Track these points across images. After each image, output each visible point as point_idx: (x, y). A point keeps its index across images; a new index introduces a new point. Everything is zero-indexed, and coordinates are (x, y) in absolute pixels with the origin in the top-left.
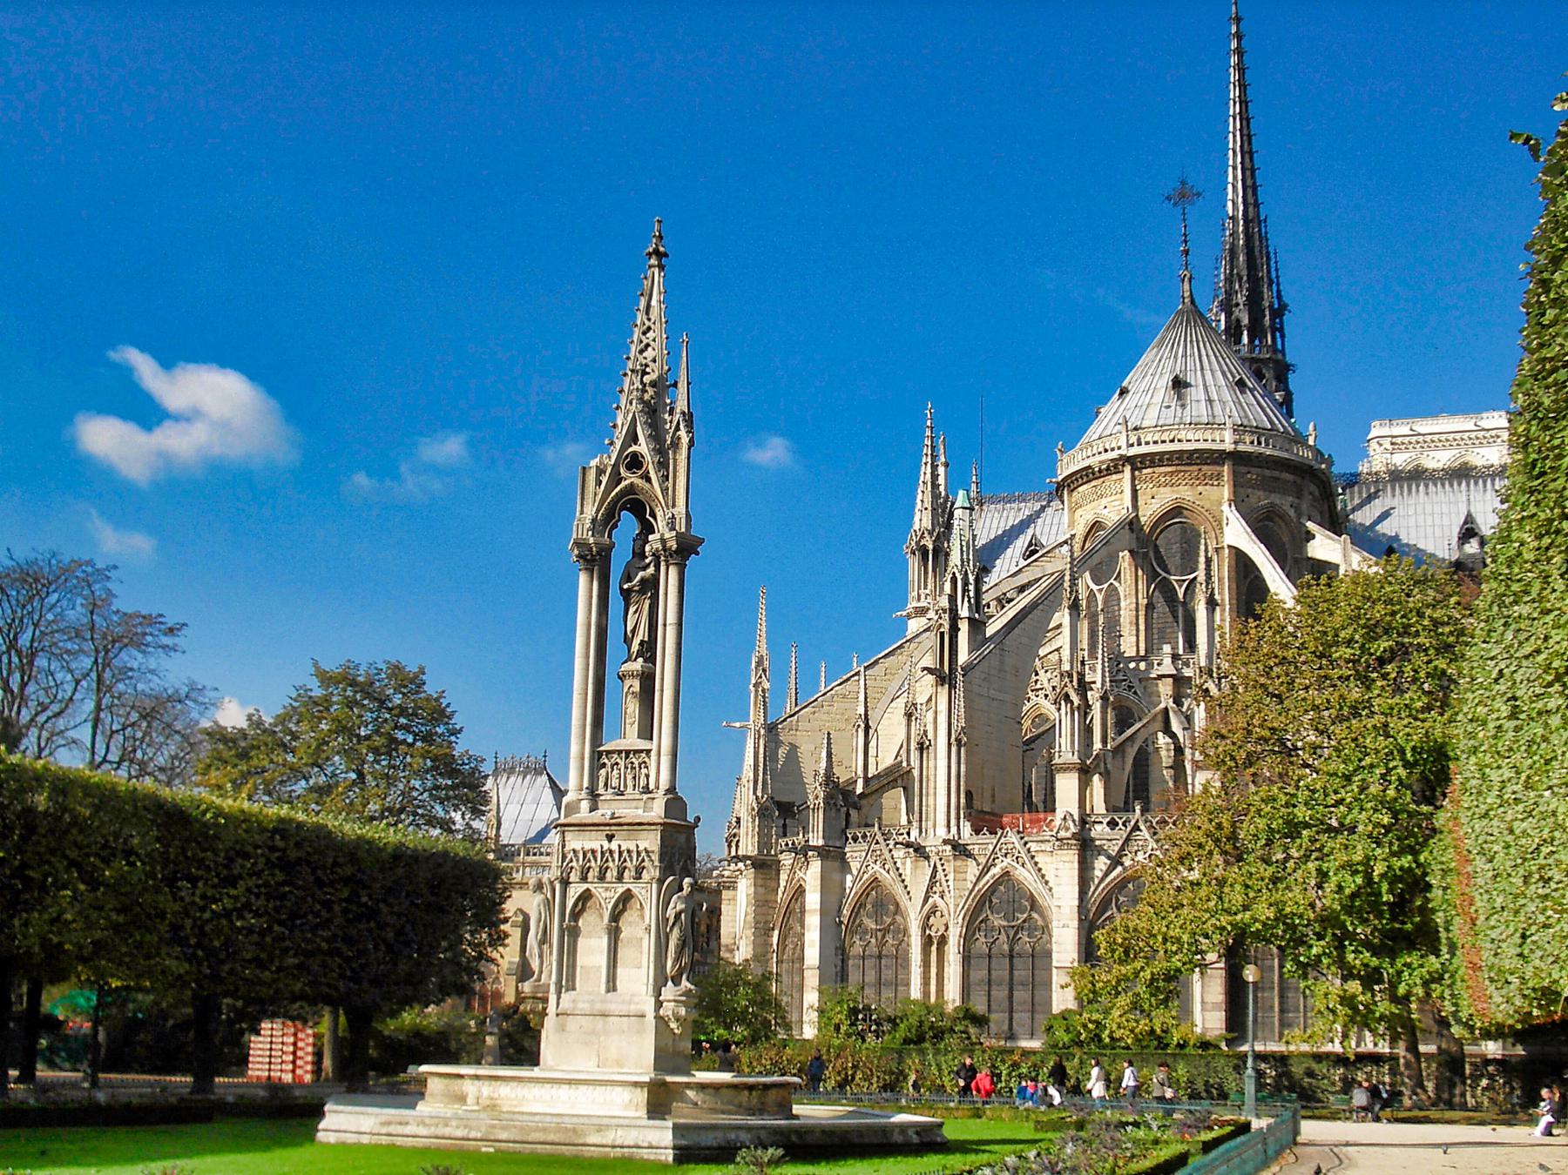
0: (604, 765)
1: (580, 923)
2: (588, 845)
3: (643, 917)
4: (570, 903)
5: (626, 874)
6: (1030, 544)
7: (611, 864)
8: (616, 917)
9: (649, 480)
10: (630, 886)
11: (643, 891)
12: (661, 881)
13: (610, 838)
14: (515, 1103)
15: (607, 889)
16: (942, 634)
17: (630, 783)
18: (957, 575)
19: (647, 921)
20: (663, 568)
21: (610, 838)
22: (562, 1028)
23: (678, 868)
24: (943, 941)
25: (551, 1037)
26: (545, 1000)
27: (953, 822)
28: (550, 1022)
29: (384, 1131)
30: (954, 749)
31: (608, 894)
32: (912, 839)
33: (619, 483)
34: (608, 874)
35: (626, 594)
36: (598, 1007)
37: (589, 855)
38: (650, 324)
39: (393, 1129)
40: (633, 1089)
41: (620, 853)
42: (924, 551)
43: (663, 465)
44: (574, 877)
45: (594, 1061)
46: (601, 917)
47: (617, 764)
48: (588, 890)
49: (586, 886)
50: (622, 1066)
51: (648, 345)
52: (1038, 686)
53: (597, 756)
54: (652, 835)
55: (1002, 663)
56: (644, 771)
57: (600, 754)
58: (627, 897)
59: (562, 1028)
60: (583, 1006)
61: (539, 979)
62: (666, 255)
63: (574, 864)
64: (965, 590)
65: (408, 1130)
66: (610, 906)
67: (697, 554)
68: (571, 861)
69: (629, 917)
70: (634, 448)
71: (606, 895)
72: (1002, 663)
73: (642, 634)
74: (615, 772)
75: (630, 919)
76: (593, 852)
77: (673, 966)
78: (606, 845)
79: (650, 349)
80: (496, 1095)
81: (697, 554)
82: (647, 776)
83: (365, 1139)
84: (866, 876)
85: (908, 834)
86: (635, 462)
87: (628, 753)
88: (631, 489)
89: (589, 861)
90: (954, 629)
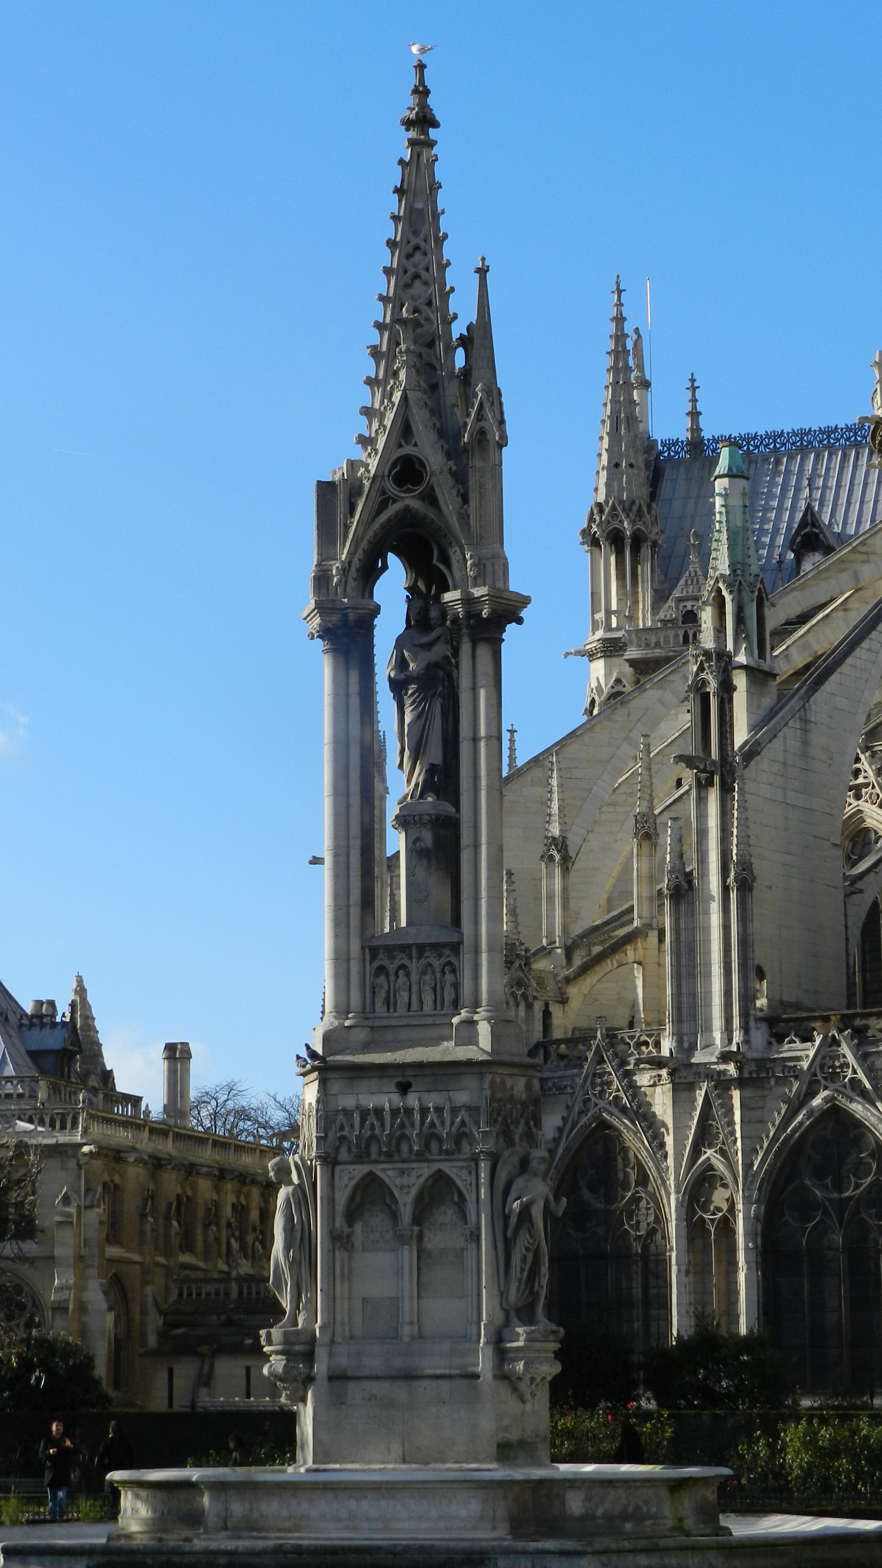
0: (381, 970)
1: (358, 1227)
4: (342, 1198)
5: (434, 1146)
6: (803, 523)
8: (418, 1219)
9: (430, 498)
11: (464, 1174)
12: (495, 1159)
13: (404, 1088)
14: (288, 1525)
15: (402, 1172)
16: (705, 698)
17: (428, 998)
18: (725, 593)
19: (472, 1219)
20: (466, 648)
21: (404, 1088)
23: (518, 1132)
24: (726, 1226)
26: (309, 1357)
27: (736, 1022)
30: (733, 896)
31: (405, 1181)
32: (665, 1052)
34: (405, 1148)
35: (398, 687)
36: (398, 1363)
37: (372, 1119)
38: (414, 241)
41: (424, 1111)
42: (616, 539)
43: (460, 478)
44: (344, 1155)
45: (396, 1449)
46: (394, 1216)
47: (403, 967)
48: (371, 1173)
51: (417, 276)
52: (860, 780)
54: (472, 1082)
55: (805, 743)
56: (449, 978)
57: (374, 952)
58: (440, 1179)
62: (435, 124)
63: (345, 1133)
64: (740, 619)
67: (520, 621)
68: (342, 1128)
69: (445, 1215)
72: (805, 743)
73: (435, 753)
74: (402, 978)
75: (442, 1219)
76: (378, 1112)
78: (396, 1099)
79: (418, 283)
80: (256, 1515)
81: (520, 621)
82: (456, 986)
84: (584, 1120)
85: (657, 1044)
87: (422, 948)
88: (407, 517)
89: (372, 1127)
90: (727, 688)
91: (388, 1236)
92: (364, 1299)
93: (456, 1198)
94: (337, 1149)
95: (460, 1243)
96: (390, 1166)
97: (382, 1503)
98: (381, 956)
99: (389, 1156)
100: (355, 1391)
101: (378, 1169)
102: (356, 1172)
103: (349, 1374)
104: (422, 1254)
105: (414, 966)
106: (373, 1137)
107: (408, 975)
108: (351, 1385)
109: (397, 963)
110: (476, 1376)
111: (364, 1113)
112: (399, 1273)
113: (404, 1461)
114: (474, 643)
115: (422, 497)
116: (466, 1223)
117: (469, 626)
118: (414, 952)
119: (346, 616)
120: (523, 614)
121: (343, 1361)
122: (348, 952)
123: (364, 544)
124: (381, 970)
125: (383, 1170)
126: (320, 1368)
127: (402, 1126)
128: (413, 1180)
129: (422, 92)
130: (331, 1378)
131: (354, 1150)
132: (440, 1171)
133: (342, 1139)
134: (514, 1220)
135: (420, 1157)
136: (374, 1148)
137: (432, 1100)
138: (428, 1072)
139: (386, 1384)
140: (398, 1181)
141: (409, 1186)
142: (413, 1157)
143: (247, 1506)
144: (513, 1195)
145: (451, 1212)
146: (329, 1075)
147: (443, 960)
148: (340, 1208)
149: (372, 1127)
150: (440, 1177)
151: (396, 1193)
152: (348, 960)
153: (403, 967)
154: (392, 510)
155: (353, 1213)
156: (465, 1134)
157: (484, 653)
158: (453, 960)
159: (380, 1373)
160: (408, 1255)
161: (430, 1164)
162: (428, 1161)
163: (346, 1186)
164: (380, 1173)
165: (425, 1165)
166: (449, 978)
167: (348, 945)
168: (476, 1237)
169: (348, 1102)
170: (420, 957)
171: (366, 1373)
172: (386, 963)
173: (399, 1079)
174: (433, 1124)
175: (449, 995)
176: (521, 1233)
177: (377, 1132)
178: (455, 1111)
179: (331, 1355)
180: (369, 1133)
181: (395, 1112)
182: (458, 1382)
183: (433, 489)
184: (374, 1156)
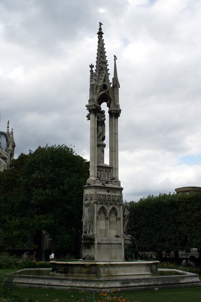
1: (99, 216)
2: (104, 193)
3: (116, 214)
4: (98, 210)
7: (110, 199)
9: (108, 92)
10: (114, 206)
13: (108, 191)
14: (115, 272)
15: (108, 207)
19: (118, 216)
22: (99, 248)
25: (96, 250)
28: (96, 246)
29: (124, 286)
31: (108, 208)
33: (101, 91)
39: (126, 285)
40: (147, 266)
44: (99, 202)
46: (105, 214)
48: (103, 206)
49: (102, 205)
50: (116, 259)
53: (98, 166)
58: (114, 209)
59: (99, 248)
60: (104, 242)
61: (89, 233)
63: (100, 198)
65: (132, 284)
66: (109, 211)
70: (105, 83)
71: (109, 209)
74: (102, 172)
76: (105, 195)
77: (126, 229)
78: (107, 194)
80: (109, 271)
81: (119, 116)
83: (119, 289)
86: (105, 87)
91: (104, 218)
92: (100, 229)
93: (115, 212)
94: (98, 201)
95: (115, 220)
96: (106, 205)
97: (131, 268)
98: (99, 168)
99: (106, 204)
100: (102, 246)
101: (104, 205)
102: (100, 206)
103: (101, 243)
104: (110, 222)
105: (104, 170)
106: (104, 200)
107: (103, 172)
108: (101, 245)
109: (101, 170)
110: (121, 244)
111: (103, 195)
112: (106, 225)
113: (110, 260)
114: (115, 118)
115: (107, 92)
116: (117, 216)
117: (115, 115)
118: (104, 168)
119: (97, 107)
120: (120, 115)
121: (99, 241)
122: (95, 166)
123: (99, 96)
124: (98, 170)
125: (105, 206)
126: (96, 242)
127: (109, 198)
128: (110, 208)
129: (100, 29)
130: (98, 244)
131: (101, 201)
132: (114, 207)
133: (99, 199)
134: (126, 217)
135: (111, 204)
136: (104, 202)
137: (114, 194)
138: (113, 189)
139: (107, 245)
140: (107, 208)
141: (109, 209)
142: (110, 204)
143: (108, 269)
144: (125, 213)
145: (114, 214)
146: (96, 188)
147: (108, 170)
148: (97, 212)
149: (104, 198)
150: (114, 209)
151: (107, 210)
152: (95, 167)
153: (102, 170)
154: (102, 92)
155: (99, 213)
156: (118, 201)
157: (116, 119)
158: (110, 170)
159: (106, 243)
160: (108, 221)
161: (113, 206)
162: (112, 205)
163: (99, 208)
164: (104, 206)
165: (111, 206)
166: (109, 173)
167: (95, 164)
168: (119, 219)
169: (99, 193)
170: (105, 169)
171: (104, 243)
172: (100, 169)
173: (108, 190)
174: (114, 199)
175: (109, 176)
176: (127, 219)
177: (105, 199)
178: (117, 196)
179: (98, 240)
180: (103, 199)
181: (108, 195)
182: (118, 245)
183: (108, 91)
184: (104, 203)
